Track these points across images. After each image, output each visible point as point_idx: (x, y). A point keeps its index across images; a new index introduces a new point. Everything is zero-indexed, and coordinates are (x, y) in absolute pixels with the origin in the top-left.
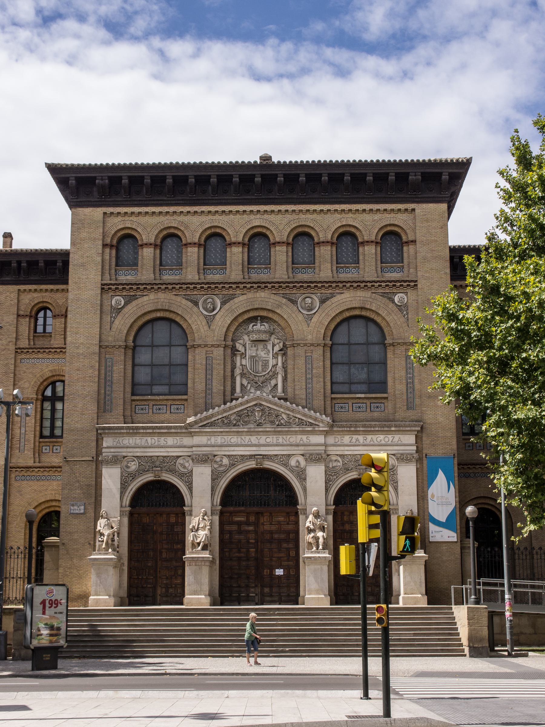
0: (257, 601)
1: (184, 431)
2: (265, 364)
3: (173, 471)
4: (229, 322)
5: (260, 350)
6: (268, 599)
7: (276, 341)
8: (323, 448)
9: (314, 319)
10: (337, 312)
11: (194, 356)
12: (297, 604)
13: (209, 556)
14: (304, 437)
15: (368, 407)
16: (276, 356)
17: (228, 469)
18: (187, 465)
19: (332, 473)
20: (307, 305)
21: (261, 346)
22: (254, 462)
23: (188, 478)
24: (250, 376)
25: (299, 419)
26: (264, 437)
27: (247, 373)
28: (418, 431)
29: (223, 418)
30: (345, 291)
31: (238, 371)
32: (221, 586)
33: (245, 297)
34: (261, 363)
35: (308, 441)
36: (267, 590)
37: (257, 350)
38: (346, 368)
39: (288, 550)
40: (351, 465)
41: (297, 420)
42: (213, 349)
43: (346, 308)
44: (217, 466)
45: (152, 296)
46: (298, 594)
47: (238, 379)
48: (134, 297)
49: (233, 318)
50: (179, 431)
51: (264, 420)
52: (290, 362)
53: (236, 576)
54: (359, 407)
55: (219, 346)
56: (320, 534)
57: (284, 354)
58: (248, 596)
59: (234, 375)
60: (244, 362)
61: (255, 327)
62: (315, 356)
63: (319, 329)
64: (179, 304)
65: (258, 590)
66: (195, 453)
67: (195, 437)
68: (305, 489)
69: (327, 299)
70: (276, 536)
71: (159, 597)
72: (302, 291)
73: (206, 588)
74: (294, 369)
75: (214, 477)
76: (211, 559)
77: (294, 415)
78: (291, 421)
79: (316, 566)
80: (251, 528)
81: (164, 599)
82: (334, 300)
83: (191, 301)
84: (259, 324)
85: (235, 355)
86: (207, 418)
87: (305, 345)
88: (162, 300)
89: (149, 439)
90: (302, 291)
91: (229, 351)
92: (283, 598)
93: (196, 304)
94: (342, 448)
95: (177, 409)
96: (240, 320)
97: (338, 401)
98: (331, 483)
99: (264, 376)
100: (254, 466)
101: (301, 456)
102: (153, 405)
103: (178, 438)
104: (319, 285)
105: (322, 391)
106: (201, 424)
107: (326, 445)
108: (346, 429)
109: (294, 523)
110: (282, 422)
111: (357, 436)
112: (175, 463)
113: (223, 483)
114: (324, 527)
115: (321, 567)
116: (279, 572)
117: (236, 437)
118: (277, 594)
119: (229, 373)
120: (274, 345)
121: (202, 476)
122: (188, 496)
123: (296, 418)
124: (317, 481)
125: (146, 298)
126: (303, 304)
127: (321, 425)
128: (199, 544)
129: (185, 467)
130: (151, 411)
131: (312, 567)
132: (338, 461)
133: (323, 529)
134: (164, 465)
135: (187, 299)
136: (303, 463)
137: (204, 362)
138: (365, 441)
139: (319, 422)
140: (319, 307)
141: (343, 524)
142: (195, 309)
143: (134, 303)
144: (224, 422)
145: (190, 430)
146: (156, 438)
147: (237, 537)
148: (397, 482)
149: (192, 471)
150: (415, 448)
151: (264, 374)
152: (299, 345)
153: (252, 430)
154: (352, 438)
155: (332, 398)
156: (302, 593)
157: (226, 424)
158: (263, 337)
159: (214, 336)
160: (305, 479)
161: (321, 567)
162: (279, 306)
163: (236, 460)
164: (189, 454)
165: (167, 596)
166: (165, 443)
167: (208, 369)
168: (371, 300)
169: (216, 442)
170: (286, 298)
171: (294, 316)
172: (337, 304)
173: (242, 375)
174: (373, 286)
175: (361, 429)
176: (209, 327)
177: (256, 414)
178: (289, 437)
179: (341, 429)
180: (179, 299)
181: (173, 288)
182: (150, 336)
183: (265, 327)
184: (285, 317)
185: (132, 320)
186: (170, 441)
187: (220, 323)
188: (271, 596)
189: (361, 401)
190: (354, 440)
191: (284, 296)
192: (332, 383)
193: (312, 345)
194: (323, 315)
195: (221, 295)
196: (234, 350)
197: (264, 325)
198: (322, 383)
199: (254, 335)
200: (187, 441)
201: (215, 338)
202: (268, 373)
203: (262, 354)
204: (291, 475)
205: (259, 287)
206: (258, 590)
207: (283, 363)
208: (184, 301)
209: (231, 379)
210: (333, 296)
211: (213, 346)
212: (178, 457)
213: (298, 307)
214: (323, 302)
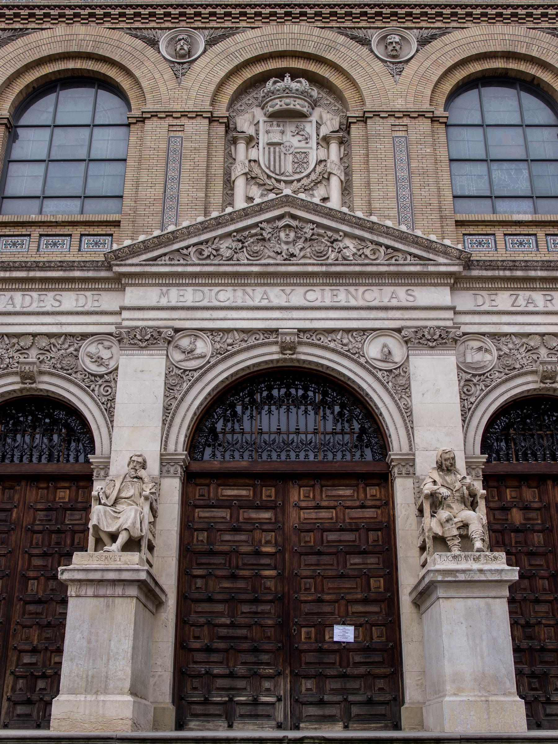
0: (280, 718)
1: (103, 274)
2: (300, 160)
3: (68, 372)
4: (222, 74)
5: (289, 134)
6: (312, 710)
7: (326, 117)
8: (449, 314)
9: (409, 70)
10: (457, 60)
11: (141, 139)
12: (397, 727)
13: (136, 567)
14: (401, 292)
15: (542, 244)
16: (324, 144)
17: (208, 362)
18: (105, 354)
19: (474, 375)
20: (390, 48)
21: (290, 128)
22: (275, 349)
23: (104, 383)
24: (268, 181)
25: (387, 247)
26: (301, 290)
27: (260, 175)
29: (201, 243)
30: (469, 24)
31: (239, 170)
32: (181, 674)
33: (257, 32)
34: (290, 158)
35: (411, 299)
36: (307, 684)
37: (283, 132)
38: (481, 168)
39: (365, 576)
40: (522, 358)
41: (383, 249)
42: (184, 121)
43: (475, 52)
44: (182, 357)
45: (61, 30)
46: (398, 699)
47: (240, 185)
48: (23, 32)
49: (230, 67)
50: (91, 274)
51: (301, 250)
52: (357, 152)
53: (221, 645)
54: (521, 244)
55: (198, 115)
56: (467, 514)
57: (341, 142)
58: (255, 703)
59: (229, 181)
60: (253, 154)
61: (278, 84)
62: (413, 137)
63: (420, 88)
64: (117, 43)
65: (284, 686)
66: (125, 323)
68: (407, 414)
69: (433, 37)
70: (332, 536)
71: (5, 704)
72: (379, 24)
73: (122, 669)
74: (367, 162)
75: (171, 381)
76: (143, 576)
77: (375, 238)
78: (367, 252)
80: (266, 515)
81: (20, 710)
82: (446, 39)
83: (143, 39)
84: (288, 79)
85: (234, 141)
86: (159, 242)
87: (392, 114)
88: (81, 37)
89: (18, 296)
90: (379, 24)
91: (221, 129)
92: (355, 710)
93: (153, 43)
94: (495, 319)
95: (96, 244)
96: (247, 74)
97: (471, 230)
98: (472, 399)
99: (299, 180)
100: (276, 357)
101: (396, 334)
102: (41, 235)
103: (88, 294)
104: (417, 11)
105: (435, 202)
106: (144, 257)
108: (501, 273)
109: (378, 503)
110: (347, 253)
111: (528, 293)
112: (77, 350)
113: (196, 398)
114: (473, 495)
116: (344, 634)
117: (230, 289)
118: (339, 698)
119: (218, 170)
120: (319, 125)
121: (141, 380)
122: (104, 430)
123: (381, 245)
124: (438, 391)
125: (45, 34)
126: (382, 48)
127: (441, 260)
128: (114, 537)
129: (99, 361)
130: (34, 246)
131: (459, 604)
132: (486, 350)
133: (471, 503)
134: (49, 355)
135: (136, 37)
136: (398, 353)
137: (164, 146)
139: (436, 252)
140: (417, 51)
141: (505, 509)
142: (150, 51)
143: (20, 42)
144: (201, 254)
145: (116, 269)
146: (35, 294)
147: (227, 537)
149: (117, 369)
151: (297, 177)
152: (377, 114)
153: (271, 269)
154: (518, 295)
155: (459, 224)
156: (412, 692)
157: (208, 257)
158: (298, 105)
159: (189, 98)
160: (407, 388)
162: (331, 48)
163: (230, 341)
164: (112, 329)
165: (29, 702)
166: (57, 304)
167: (172, 156)
168: (527, 40)
169: (182, 299)
170: (347, 35)
171: (364, 64)
172: (456, 45)
173: (250, 178)
174: (530, 15)
175: (540, 273)
176: (180, 83)
177: (282, 235)
178: (362, 289)
179: (490, 273)
180: (117, 34)
181: (107, 15)
182: (51, 109)
183: (303, 84)
184: (345, 66)
185: (12, 70)
186: (70, 300)
187: (203, 76)
188: (321, 703)
189: (525, 230)
190: (521, 301)
191: (341, 31)
192: (455, 197)
193: (407, 114)
194: (427, 64)
195: (206, 32)
196: (232, 136)
197: (300, 82)
198: (433, 189)
199: (277, 101)
200: (109, 301)
201: (191, 102)
202: (308, 176)
203: (295, 142)
205: (288, 14)
206: (284, 686)
207: (341, 159)
208: (127, 39)
209: (224, 188)
210: (444, 32)
211: (184, 114)
212: (84, 336)
213: (372, 51)
214: (423, 42)
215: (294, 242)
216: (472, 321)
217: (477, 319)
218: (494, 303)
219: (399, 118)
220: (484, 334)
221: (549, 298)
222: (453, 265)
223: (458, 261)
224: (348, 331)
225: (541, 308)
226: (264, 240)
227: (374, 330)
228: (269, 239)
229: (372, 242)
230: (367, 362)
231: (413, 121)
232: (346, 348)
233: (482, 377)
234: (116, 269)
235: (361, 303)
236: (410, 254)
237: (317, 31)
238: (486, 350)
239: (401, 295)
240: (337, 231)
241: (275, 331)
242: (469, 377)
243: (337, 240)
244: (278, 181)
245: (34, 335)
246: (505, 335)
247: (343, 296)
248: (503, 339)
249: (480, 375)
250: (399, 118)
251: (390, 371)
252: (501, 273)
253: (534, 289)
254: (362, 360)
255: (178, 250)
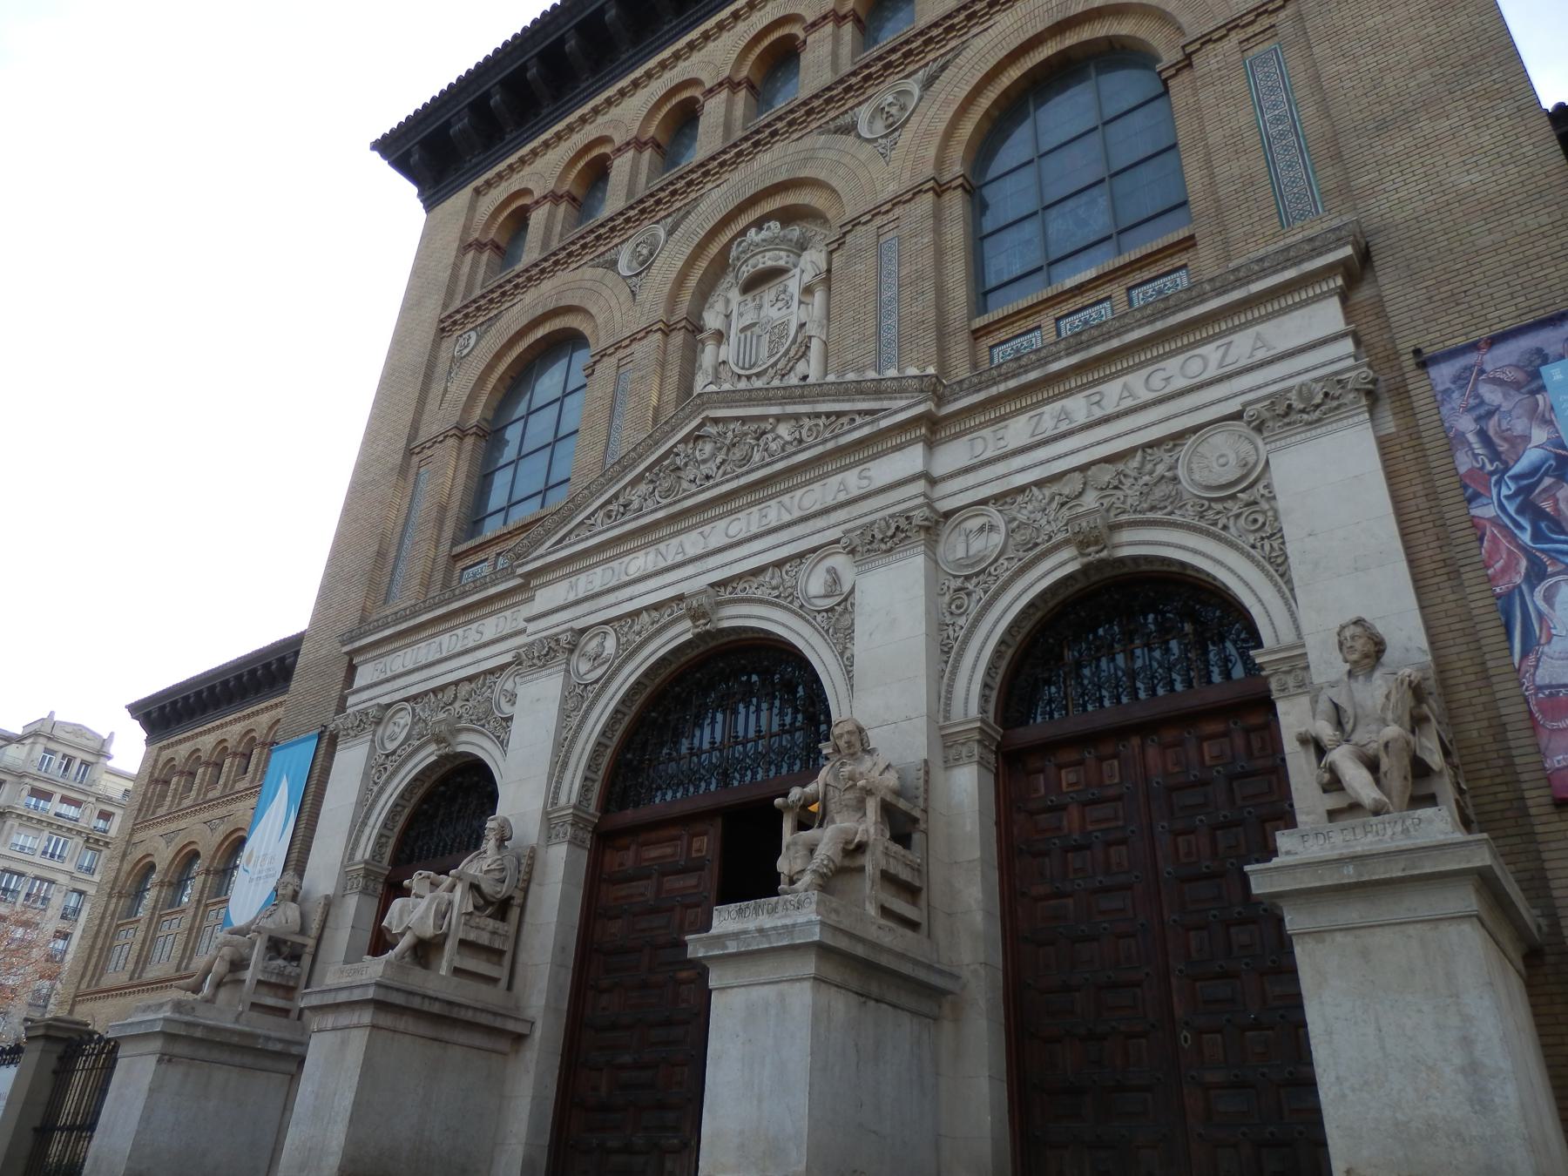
5: (766, 305)
8: (920, 486)
19: (967, 578)
21: (769, 293)
28: (1343, 264)
35: (865, 482)
37: (760, 307)
67: (538, 593)
79: (757, 993)
94: (1000, 469)
98: (961, 621)
107: (933, 481)
115: (782, 998)
123: (818, 415)
125: (518, 306)
138: (1095, 408)
143: (493, 330)
145: (520, 571)
148: (1278, 533)
150: (1348, 346)
161: (782, 998)
198: (931, 295)
204: (807, 631)
215: (714, 456)
216: (964, 486)
217: (971, 479)
218: (1002, 443)
219: (887, 212)
220: (984, 502)
221: (1097, 398)
222: (920, 403)
223: (922, 396)
224: (778, 564)
225: (1081, 418)
226: (678, 468)
227: (814, 550)
228: (686, 465)
229: (809, 415)
230: (802, 606)
231: (907, 206)
232: (776, 593)
233: (981, 577)
234: (520, 571)
235: (797, 514)
236: (859, 412)
237: (792, 148)
238: (992, 528)
239: (852, 481)
240: (764, 418)
241: (680, 598)
242: (959, 583)
243: (764, 433)
244: (749, 378)
245: (456, 683)
246: (1021, 490)
247: (774, 513)
248: (1020, 499)
249: (977, 574)
250: (887, 212)
251: (831, 610)
252: (1002, 388)
253: (1069, 393)
254: (795, 606)
255: (582, 523)
